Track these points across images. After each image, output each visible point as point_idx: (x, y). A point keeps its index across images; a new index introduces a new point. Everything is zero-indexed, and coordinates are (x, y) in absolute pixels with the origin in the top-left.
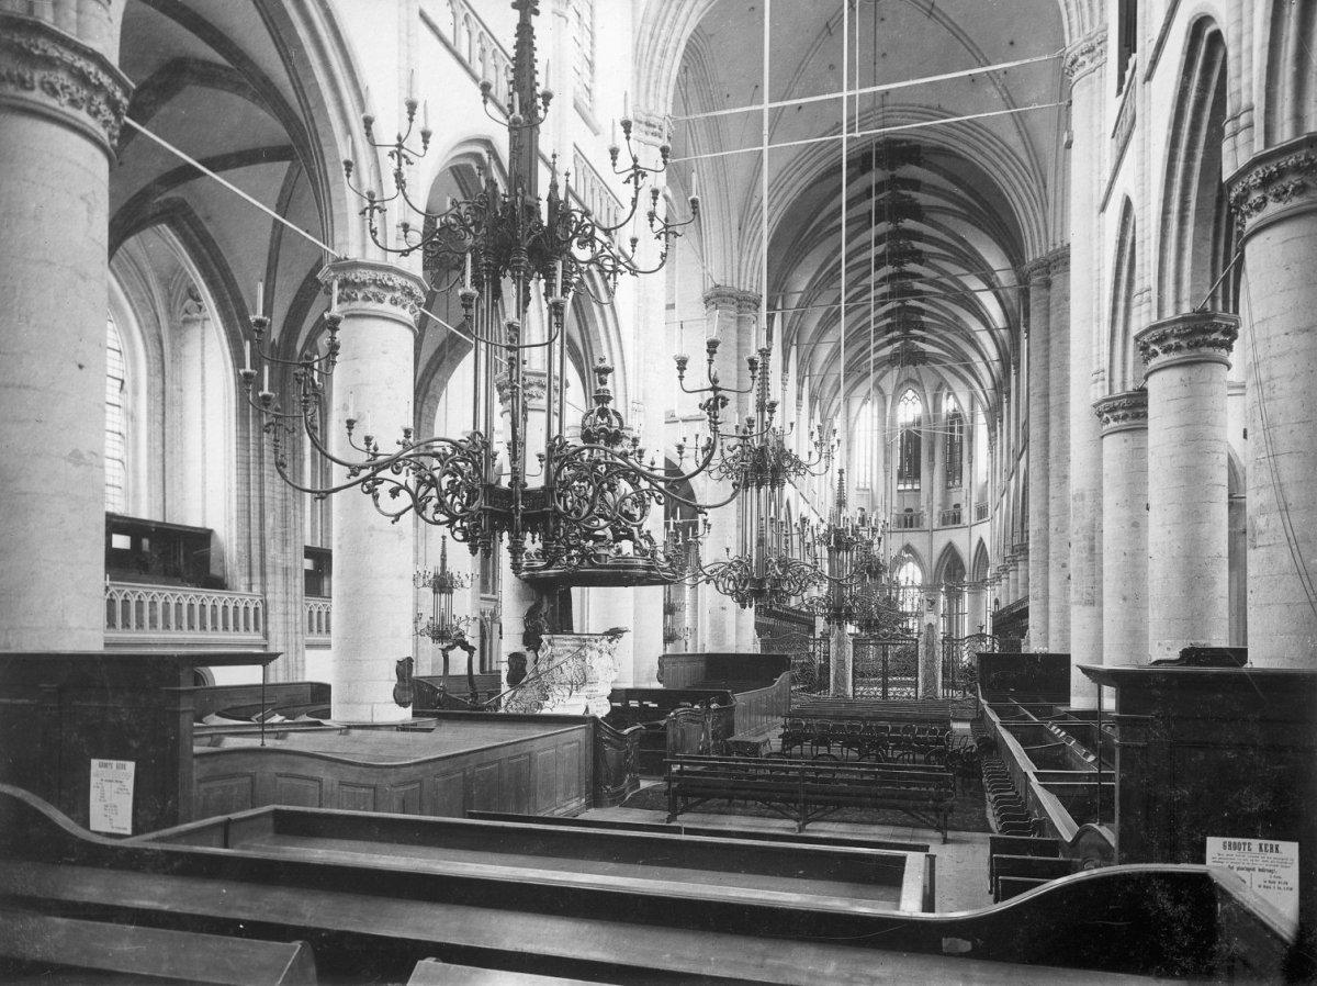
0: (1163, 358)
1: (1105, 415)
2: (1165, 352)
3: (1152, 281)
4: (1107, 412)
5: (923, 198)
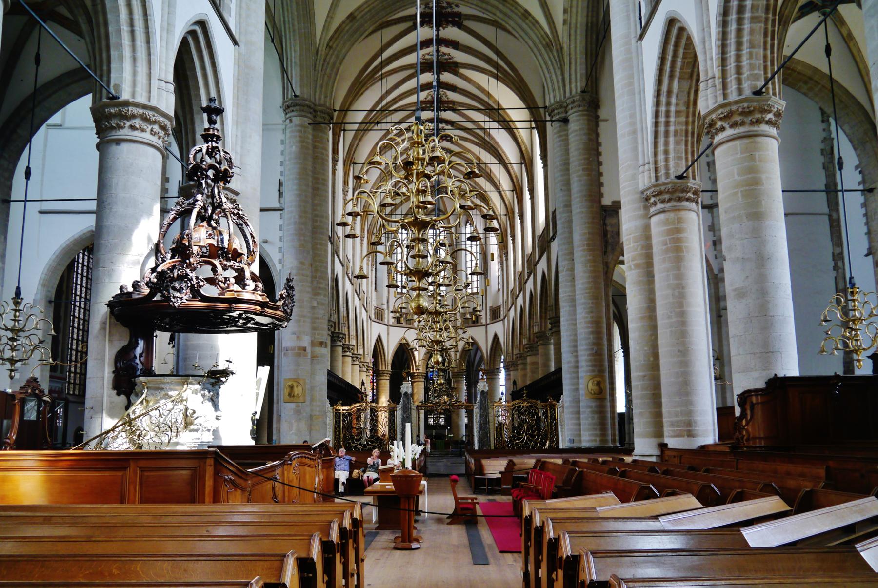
0: (729, 132)
1: (652, 200)
2: (731, 127)
3: (717, 72)
4: (654, 196)
5: (459, 56)
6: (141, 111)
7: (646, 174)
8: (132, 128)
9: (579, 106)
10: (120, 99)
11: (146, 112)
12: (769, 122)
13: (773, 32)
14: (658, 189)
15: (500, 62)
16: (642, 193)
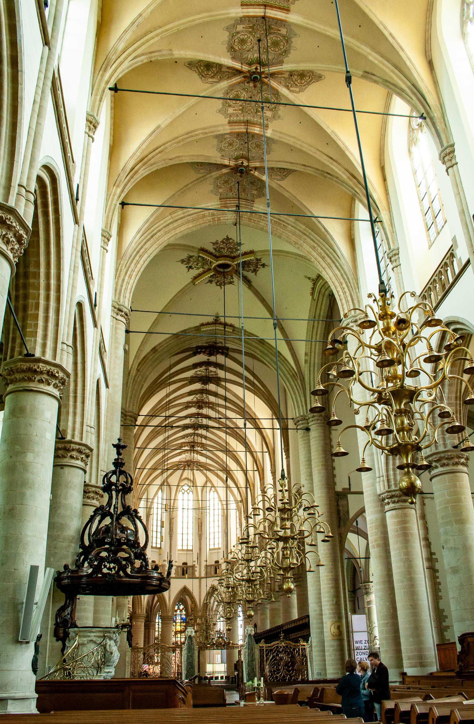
0: (440, 469)
1: (386, 501)
6: (78, 447)
7: (381, 483)
8: (72, 457)
9: (318, 420)
10: (66, 439)
11: (81, 447)
12: (463, 464)
13: (460, 410)
14: (390, 494)
15: (256, 382)
16: (380, 495)
